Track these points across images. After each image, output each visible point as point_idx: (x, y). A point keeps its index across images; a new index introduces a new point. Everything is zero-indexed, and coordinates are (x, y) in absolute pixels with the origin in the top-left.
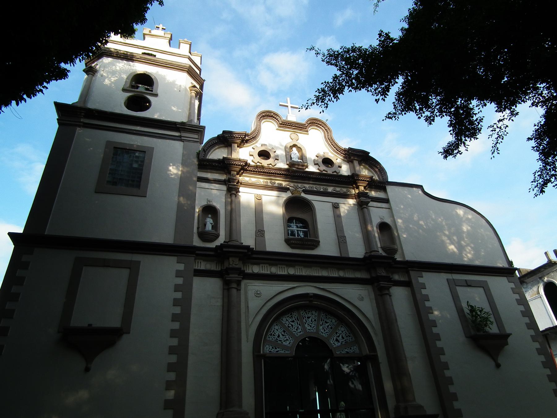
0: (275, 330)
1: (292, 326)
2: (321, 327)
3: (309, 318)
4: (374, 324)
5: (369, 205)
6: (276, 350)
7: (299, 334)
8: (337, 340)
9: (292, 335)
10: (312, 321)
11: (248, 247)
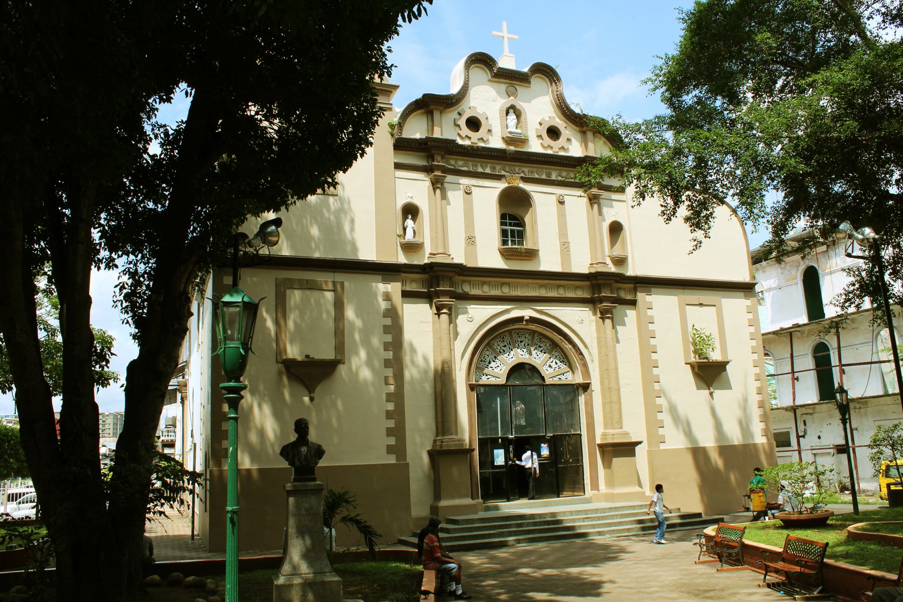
0: (486, 356)
1: (504, 351)
3: (521, 342)
5: (601, 197)
7: (511, 360)
8: (550, 366)
10: (525, 345)
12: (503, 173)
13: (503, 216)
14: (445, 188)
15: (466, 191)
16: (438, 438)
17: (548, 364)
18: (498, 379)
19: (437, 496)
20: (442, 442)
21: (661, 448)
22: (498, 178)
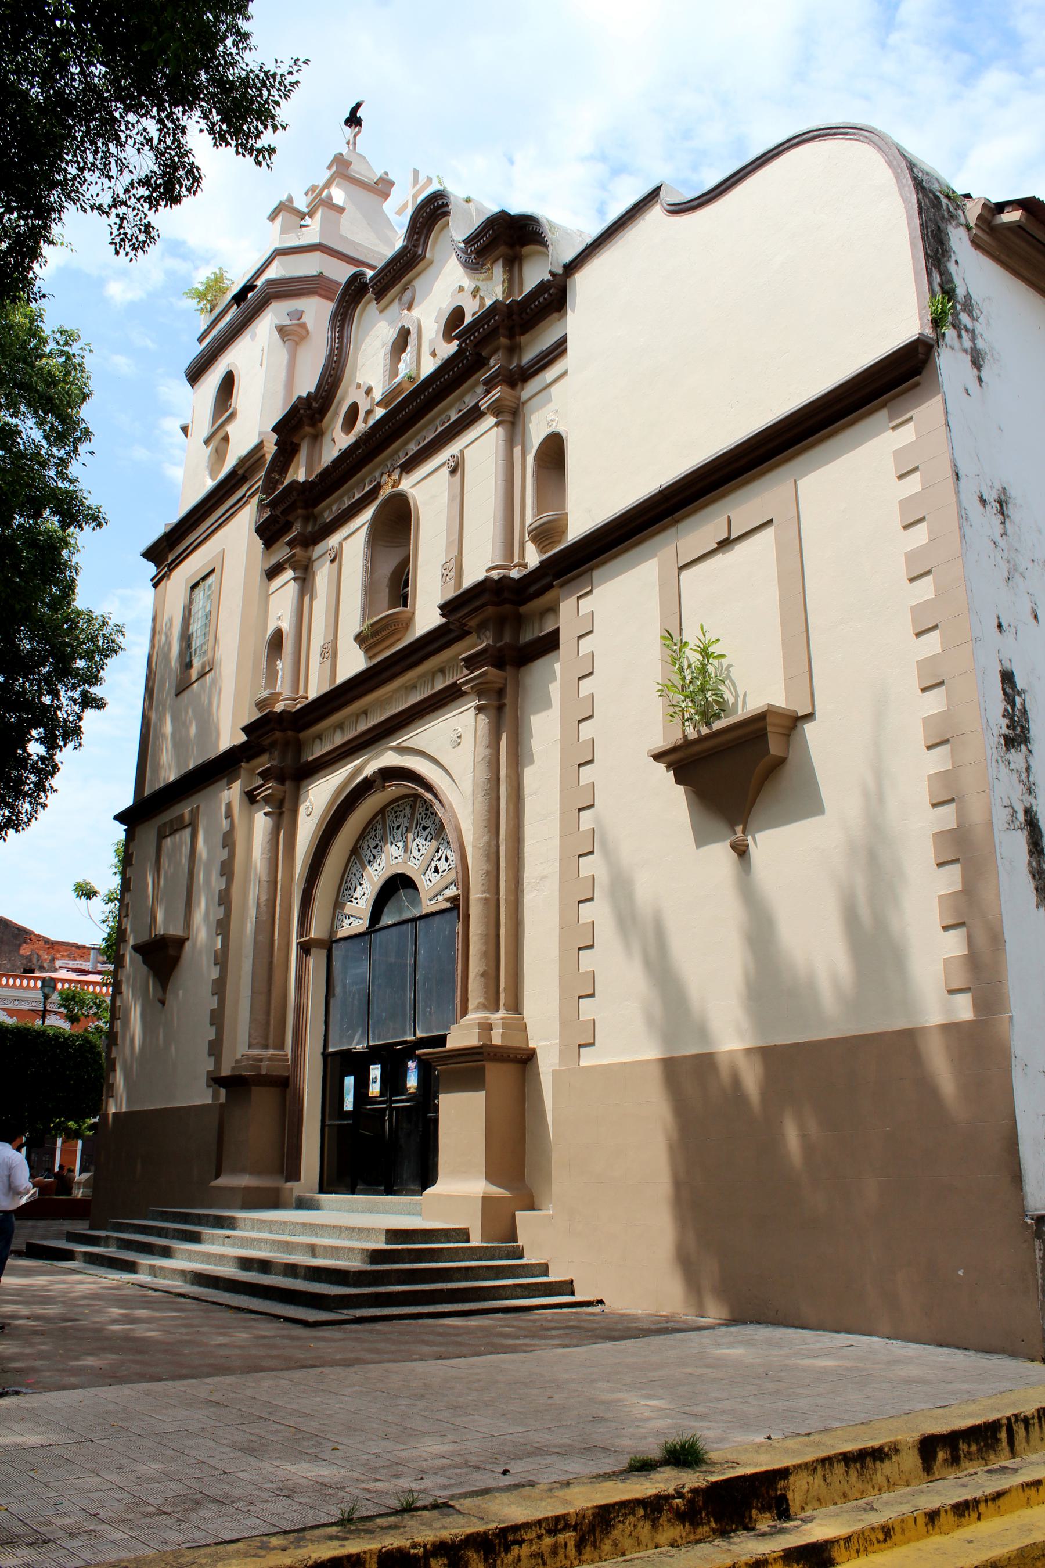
1: (374, 856)
8: (436, 871)
17: (433, 864)
21: (583, 1064)
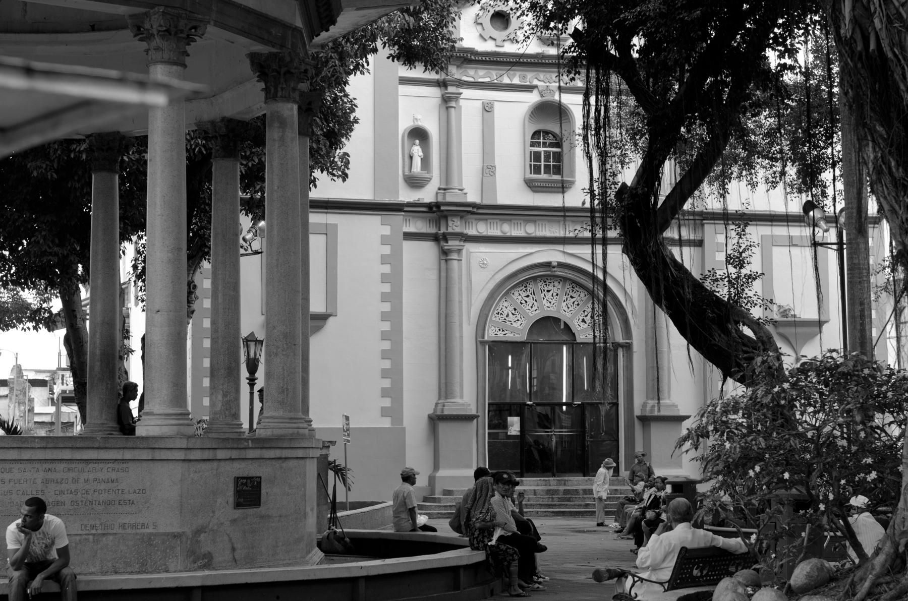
0: (504, 308)
1: (526, 302)
2: (564, 304)
3: (548, 291)
4: (636, 303)
6: (504, 333)
8: (583, 321)
9: (525, 316)
11: (473, 205)
12: (536, 82)
13: (536, 134)
14: (461, 107)
15: (487, 109)
16: (440, 401)
18: (517, 336)
19: (436, 467)
20: (444, 406)
22: (529, 88)
